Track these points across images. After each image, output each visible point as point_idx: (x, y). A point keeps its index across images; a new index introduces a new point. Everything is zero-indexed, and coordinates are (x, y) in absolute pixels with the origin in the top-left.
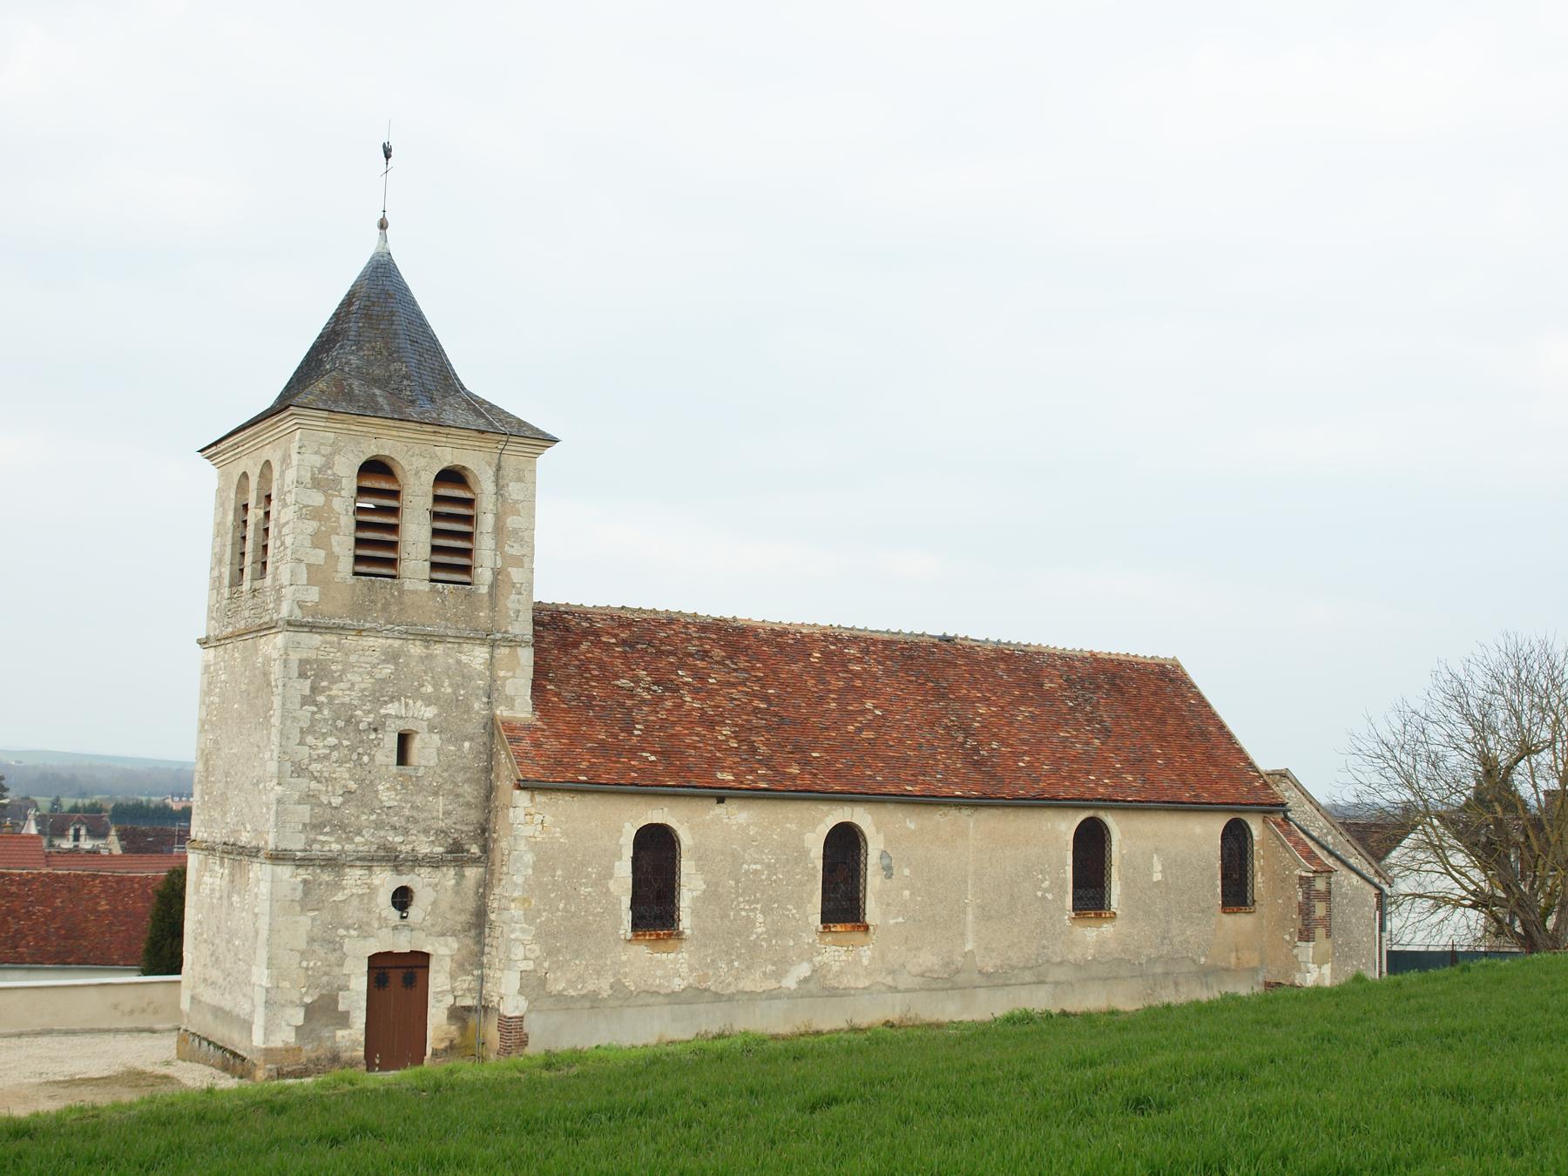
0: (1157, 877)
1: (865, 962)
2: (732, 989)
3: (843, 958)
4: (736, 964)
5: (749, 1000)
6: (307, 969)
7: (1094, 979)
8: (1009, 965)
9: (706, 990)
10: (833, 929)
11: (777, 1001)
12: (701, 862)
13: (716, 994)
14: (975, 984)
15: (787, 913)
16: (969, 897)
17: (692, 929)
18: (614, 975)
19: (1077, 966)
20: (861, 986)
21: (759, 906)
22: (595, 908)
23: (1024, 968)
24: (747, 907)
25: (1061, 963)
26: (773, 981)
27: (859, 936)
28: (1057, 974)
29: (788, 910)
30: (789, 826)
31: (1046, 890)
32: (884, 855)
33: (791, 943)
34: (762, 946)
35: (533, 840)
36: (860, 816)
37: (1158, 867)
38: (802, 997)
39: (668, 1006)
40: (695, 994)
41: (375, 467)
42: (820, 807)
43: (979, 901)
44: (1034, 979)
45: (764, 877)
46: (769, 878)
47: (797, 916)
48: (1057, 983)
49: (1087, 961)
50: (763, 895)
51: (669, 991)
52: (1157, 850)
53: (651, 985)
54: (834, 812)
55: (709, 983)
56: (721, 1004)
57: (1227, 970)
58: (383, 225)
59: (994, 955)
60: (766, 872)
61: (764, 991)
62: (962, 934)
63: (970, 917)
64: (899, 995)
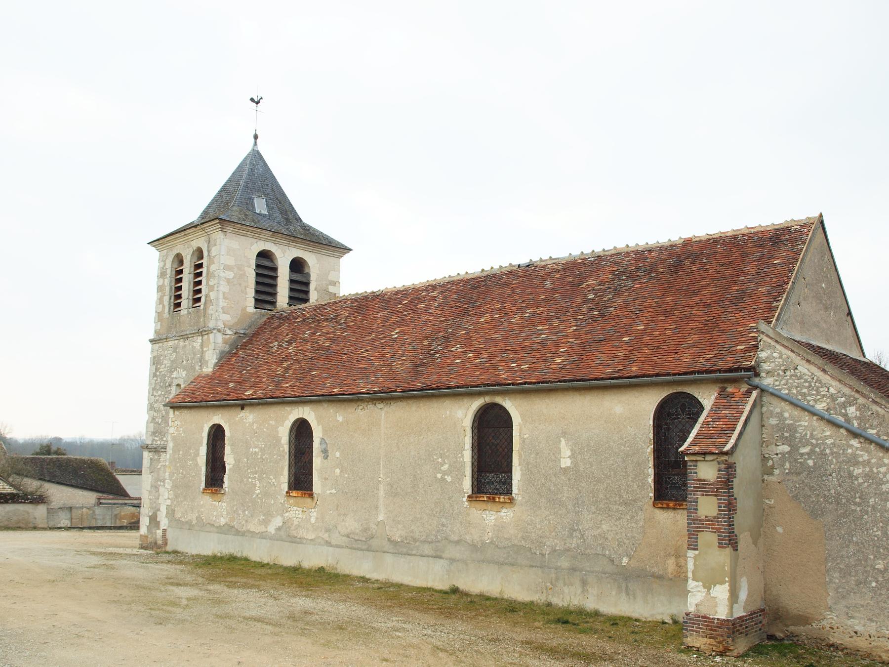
0: (566, 463)
1: (313, 520)
2: (244, 529)
3: (300, 516)
4: (247, 512)
5: (251, 537)
6: (150, 499)
7: (489, 562)
8: (412, 537)
9: (233, 527)
10: (291, 494)
11: (265, 540)
12: (233, 447)
13: (237, 530)
14: (385, 549)
15: (270, 481)
16: (381, 476)
17: (228, 488)
18: (198, 513)
19: (474, 547)
20: (310, 538)
21: (257, 476)
22: (192, 473)
23: (425, 542)
24: (252, 476)
25: (458, 542)
26: (263, 526)
27: (309, 500)
28: (452, 551)
29: (270, 479)
30: (271, 422)
31: (445, 473)
32: (323, 440)
33: (272, 502)
34: (258, 502)
35: (173, 435)
36: (307, 413)
37: (566, 452)
38: (277, 540)
39: (217, 534)
40: (228, 529)
41: (264, 255)
42: (286, 408)
43: (388, 479)
44: (432, 553)
45: (259, 457)
46: (261, 458)
47: (275, 483)
48: (452, 560)
49: (484, 544)
50: (258, 469)
51: (218, 525)
52: (564, 434)
53: (212, 520)
54: (293, 411)
55: (235, 523)
56: (239, 537)
57: (660, 577)
58: (256, 137)
59: (400, 526)
60: (260, 454)
61: (259, 532)
62: (377, 507)
63: (382, 493)
64: (331, 549)
